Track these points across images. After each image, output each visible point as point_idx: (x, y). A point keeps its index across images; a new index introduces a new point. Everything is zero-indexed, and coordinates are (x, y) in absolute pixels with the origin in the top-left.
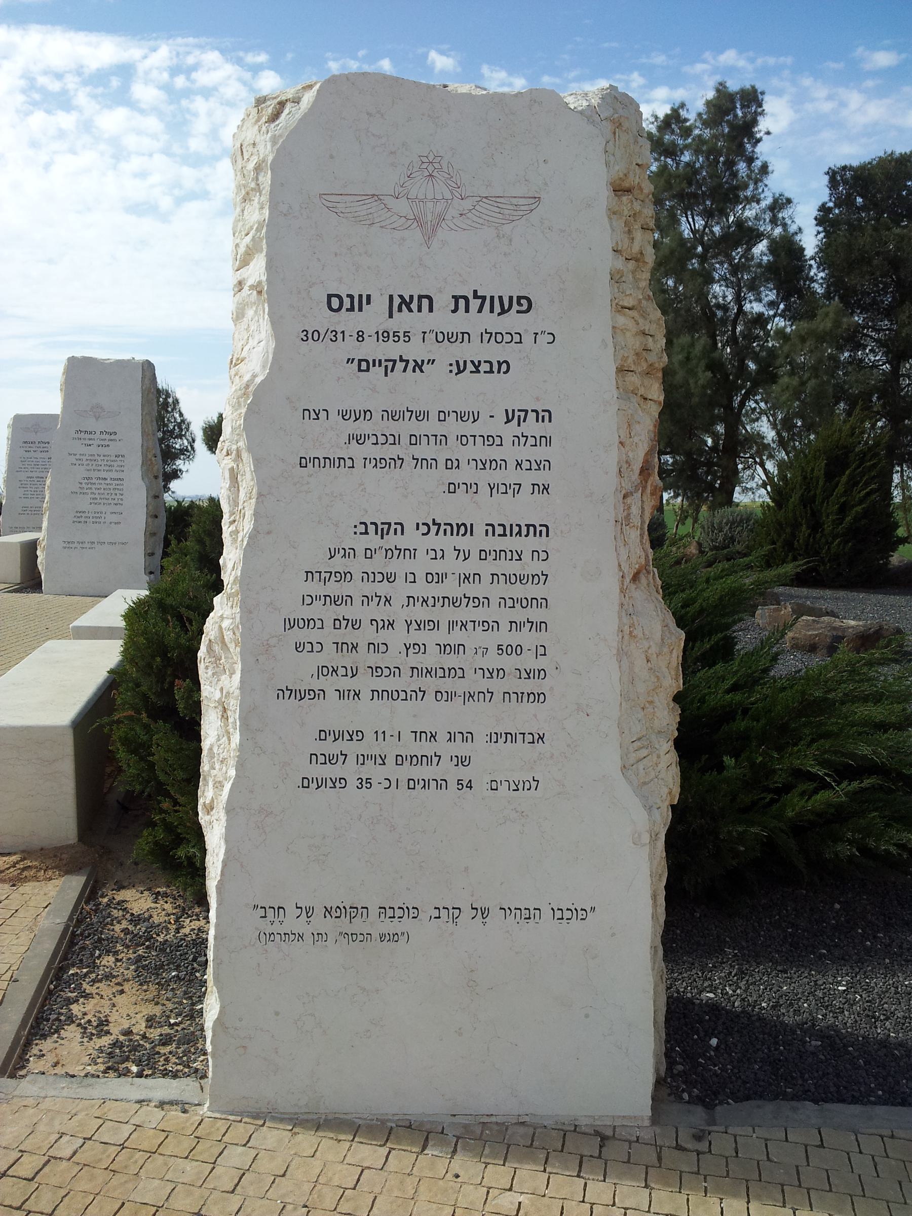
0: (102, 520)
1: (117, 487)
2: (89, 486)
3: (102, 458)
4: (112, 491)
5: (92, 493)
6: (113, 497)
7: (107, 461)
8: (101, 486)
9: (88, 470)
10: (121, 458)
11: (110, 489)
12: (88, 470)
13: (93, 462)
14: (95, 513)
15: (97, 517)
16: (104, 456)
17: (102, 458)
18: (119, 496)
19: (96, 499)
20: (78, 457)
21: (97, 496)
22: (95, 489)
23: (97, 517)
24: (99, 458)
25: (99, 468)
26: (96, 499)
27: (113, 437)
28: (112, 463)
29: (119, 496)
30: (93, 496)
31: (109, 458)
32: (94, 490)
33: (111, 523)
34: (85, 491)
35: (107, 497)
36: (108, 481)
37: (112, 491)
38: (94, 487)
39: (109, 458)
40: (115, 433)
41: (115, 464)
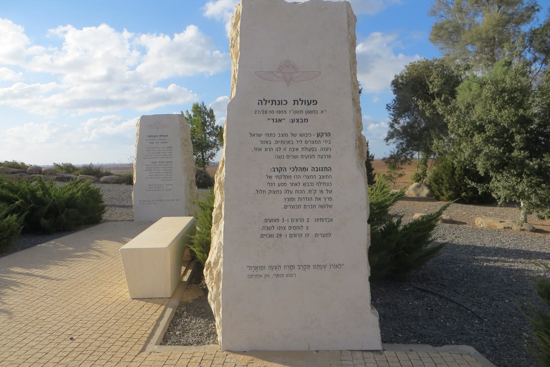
0: (304, 231)
1: (322, 181)
2: (283, 181)
3: (298, 138)
4: (316, 187)
5: (287, 191)
6: (318, 195)
7: (306, 142)
8: (299, 180)
9: (279, 157)
10: (325, 138)
11: (312, 184)
12: (279, 157)
13: (286, 145)
15: (295, 228)
16: (301, 135)
17: (298, 138)
19: (293, 199)
20: (264, 138)
23: (295, 228)
24: (294, 139)
25: (295, 153)
26: (293, 199)
27: (312, 107)
28: (314, 146)
30: (289, 196)
31: (308, 139)
32: (289, 187)
34: (276, 188)
35: (309, 196)
36: (310, 173)
37: (316, 187)
38: (288, 181)
39: (308, 139)
41: (318, 146)
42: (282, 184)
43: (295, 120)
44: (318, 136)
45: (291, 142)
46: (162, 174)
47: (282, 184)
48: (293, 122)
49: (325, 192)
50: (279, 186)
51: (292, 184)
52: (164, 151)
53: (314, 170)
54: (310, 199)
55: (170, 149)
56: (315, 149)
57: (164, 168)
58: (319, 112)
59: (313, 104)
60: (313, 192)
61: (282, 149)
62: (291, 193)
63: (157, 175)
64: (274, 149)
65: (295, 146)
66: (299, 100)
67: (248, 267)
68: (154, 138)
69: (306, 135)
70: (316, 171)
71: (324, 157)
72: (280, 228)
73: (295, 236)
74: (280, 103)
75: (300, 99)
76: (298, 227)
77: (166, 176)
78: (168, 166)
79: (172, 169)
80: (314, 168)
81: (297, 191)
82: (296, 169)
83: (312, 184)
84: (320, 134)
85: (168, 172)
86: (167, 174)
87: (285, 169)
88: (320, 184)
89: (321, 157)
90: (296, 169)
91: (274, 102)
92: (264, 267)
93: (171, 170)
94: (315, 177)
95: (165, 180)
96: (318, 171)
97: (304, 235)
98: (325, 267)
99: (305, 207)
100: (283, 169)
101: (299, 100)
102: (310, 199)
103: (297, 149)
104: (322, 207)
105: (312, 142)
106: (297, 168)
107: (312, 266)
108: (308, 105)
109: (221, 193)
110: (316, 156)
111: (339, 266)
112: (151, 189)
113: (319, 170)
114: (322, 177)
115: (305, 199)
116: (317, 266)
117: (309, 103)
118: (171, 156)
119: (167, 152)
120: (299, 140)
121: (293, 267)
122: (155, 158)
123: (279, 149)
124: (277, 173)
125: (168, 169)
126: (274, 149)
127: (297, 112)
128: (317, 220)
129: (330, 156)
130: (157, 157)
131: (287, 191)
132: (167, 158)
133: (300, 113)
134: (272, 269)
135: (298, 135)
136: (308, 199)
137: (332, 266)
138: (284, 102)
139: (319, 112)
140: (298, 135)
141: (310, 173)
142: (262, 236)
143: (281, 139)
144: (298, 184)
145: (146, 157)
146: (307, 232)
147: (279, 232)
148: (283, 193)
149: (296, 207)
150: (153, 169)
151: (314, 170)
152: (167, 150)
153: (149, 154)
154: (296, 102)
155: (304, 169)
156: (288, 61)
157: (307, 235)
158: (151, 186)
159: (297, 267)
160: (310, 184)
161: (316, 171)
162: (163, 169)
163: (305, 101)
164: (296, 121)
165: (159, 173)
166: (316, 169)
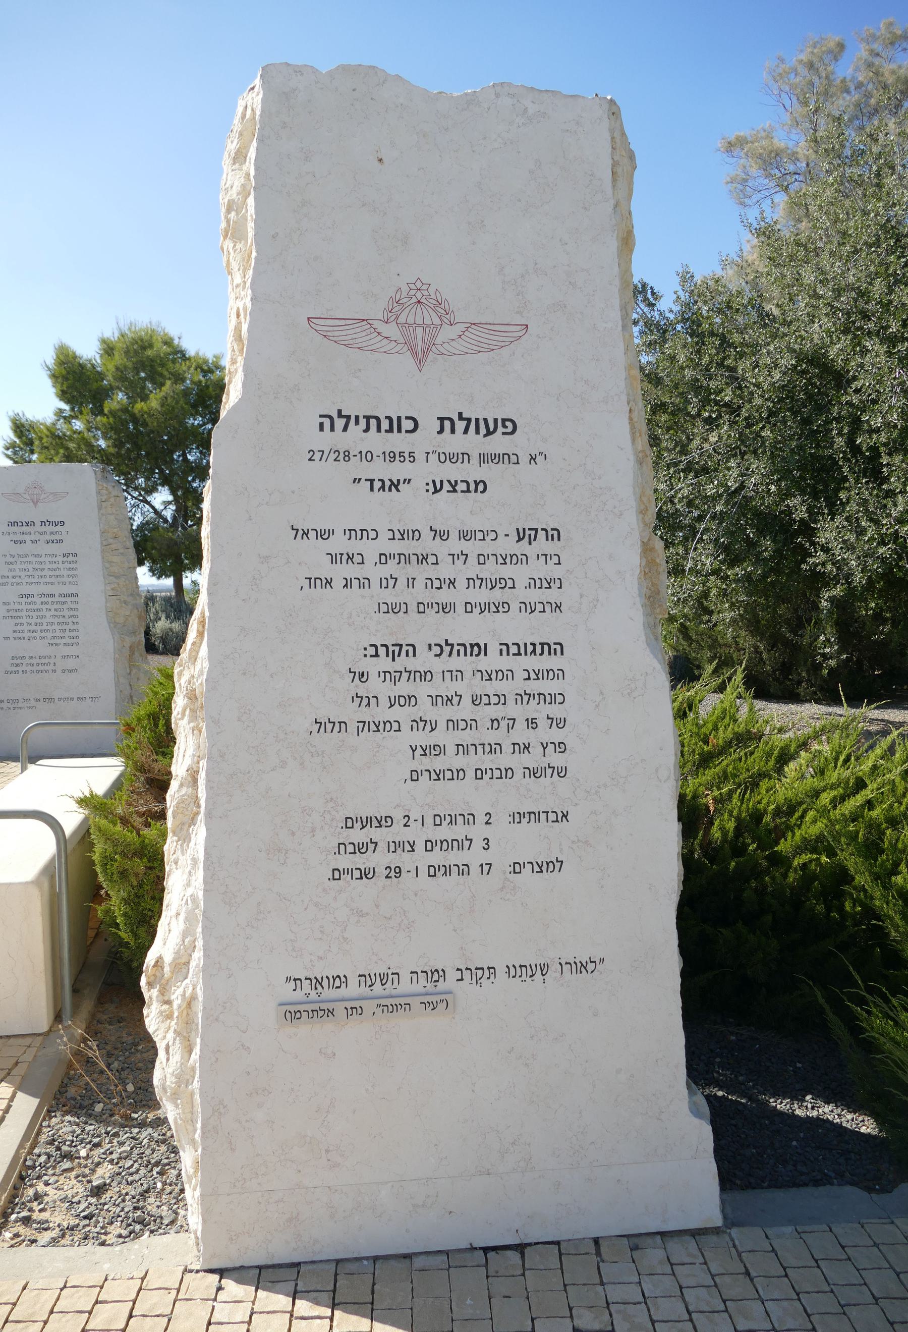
0: (474, 856)
1: (534, 687)
2: (404, 688)
3: (455, 545)
4: (512, 710)
5: (419, 723)
6: (521, 734)
7: (482, 559)
9: (392, 609)
10: (542, 544)
11: (502, 699)
12: (392, 609)
13: (413, 570)
14: (438, 821)
15: (447, 845)
16: (465, 535)
17: (455, 545)
18: (546, 733)
19: (438, 750)
20: (339, 544)
21: (441, 737)
22: (434, 700)
23: (447, 845)
24: (442, 549)
25: (445, 596)
27: (499, 443)
28: (507, 571)
29: (546, 733)
30: (423, 738)
31: (488, 548)
32: (425, 709)
33: (517, 868)
34: (383, 713)
35: (491, 737)
36: (493, 661)
37: (512, 710)
38: (422, 690)
39: (488, 548)
40: (510, 426)
41: (520, 574)
42: (402, 700)
43: (446, 484)
44: (520, 540)
45: (431, 559)
46: (49, 627)
47: (402, 700)
48: (436, 491)
49: (543, 723)
50: (392, 706)
51: (434, 700)
52: (54, 566)
53: (508, 654)
54: (494, 749)
55: (71, 558)
56: (510, 583)
57: (56, 610)
58: (524, 459)
59: (504, 433)
60: (503, 724)
61: (402, 582)
62: (433, 730)
63: (35, 631)
64: (375, 583)
65: (446, 570)
66: (456, 418)
67: (288, 979)
68: (25, 529)
69: (480, 535)
70: (514, 655)
71: (540, 607)
72: (396, 846)
73: (447, 871)
74: (395, 425)
75: (460, 414)
76: (455, 843)
77: (62, 634)
78: (65, 606)
79: (75, 613)
80: (507, 645)
81: (451, 723)
82: (447, 649)
83: (502, 698)
84: (527, 532)
85: (67, 624)
86: (64, 627)
87: (411, 649)
88: (526, 698)
89: (529, 610)
90: (447, 649)
91: (373, 422)
92: (343, 979)
93: (74, 616)
94: (510, 673)
95: (57, 645)
96: (519, 654)
97: (475, 869)
98: (544, 969)
99: (479, 775)
100: (405, 648)
101: (456, 418)
102: (494, 749)
103: (452, 583)
104: (535, 773)
105: (500, 560)
106: (452, 645)
107: (501, 971)
108: (485, 436)
109: (196, 730)
110: (515, 606)
111: (591, 967)
112: (20, 669)
113: (522, 651)
114: (533, 676)
115: (480, 748)
116: (518, 969)
117: (492, 429)
118: (75, 580)
119: (61, 566)
120: (457, 551)
121: (441, 973)
122: (30, 584)
123: (391, 582)
124: (384, 663)
125: (67, 613)
126: (375, 583)
127: (452, 458)
128: (518, 817)
129: (559, 607)
130: (36, 580)
131: (419, 723)
132: (64, 583)
133: (460, 460)
134: (369, 983)
135: (454, 535)
136: (487, 748)
137: (566, 968)
138: (407, 425)
139: (524, 459)
140: (454, 535)
141: (493, 661)
142: (337, 876)
143: (397, 547)
144: (456, 700)
145: (5, 580)
146: (486, 857)
147: (393, 859)
148: (405, 727)
149: (448, 775)
150: (23, 614)
151: (508, 654)
152: (63, 562)
153: (14, 574)
154: (447, 424)
155: (476, 649)
156: (419, 284)
157: (486, 868)
158: (19, 661)
159: (452, 975)
160: (494, 700)
161: (514, 655)
162: (53, 613)
163: (477, 420)
164: (447, 486)
165: (41, 624)
166: (514, 650)
